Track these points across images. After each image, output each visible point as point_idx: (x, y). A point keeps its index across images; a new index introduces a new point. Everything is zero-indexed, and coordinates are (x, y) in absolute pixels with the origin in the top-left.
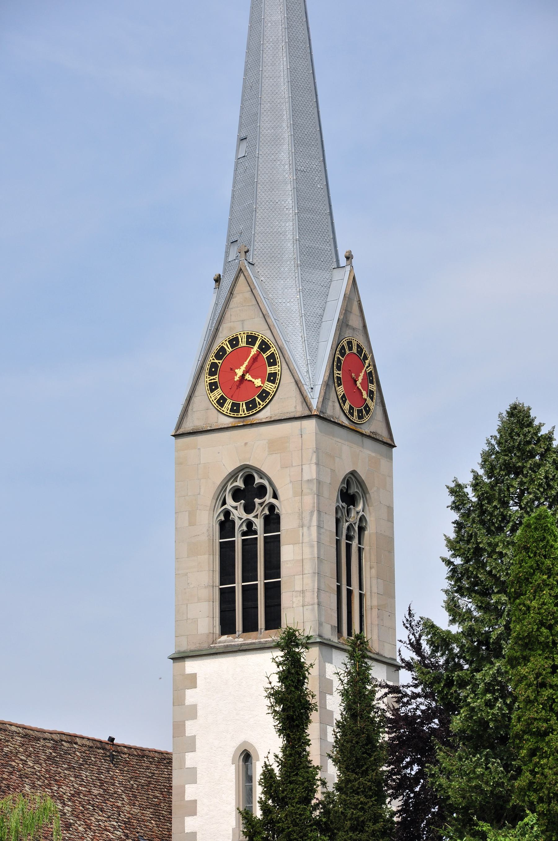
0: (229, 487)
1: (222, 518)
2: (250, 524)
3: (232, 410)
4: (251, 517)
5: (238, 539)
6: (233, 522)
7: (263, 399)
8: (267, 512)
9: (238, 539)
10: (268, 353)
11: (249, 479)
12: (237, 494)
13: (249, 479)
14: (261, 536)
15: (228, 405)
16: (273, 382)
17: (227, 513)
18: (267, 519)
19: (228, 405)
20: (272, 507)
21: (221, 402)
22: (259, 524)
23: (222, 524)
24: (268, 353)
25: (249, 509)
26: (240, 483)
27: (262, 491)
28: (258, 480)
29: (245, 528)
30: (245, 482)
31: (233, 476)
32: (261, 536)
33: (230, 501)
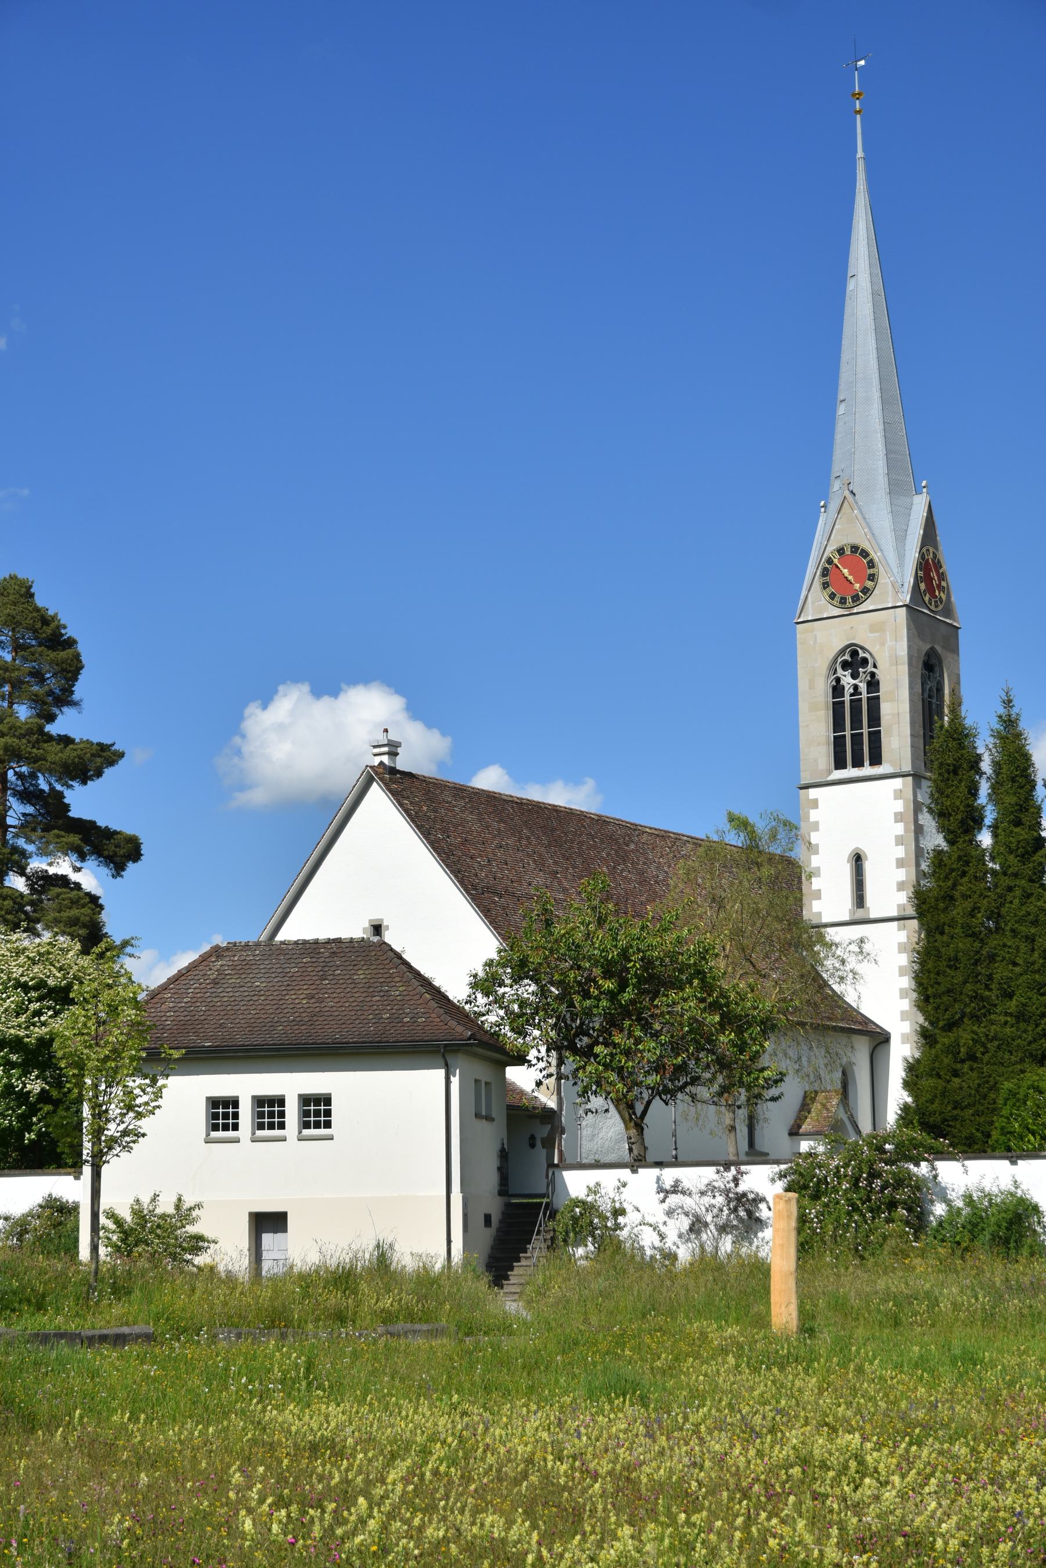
0: (840, 660)
1: (834, 683)
2: (856, 687)
3: (841, 603)
5: (847, 698)
6: (843, 687)
7: (865, 593)
8: (869, 678)
9: (847, 698)
10: (868, 559)
11: (854, 654)
12: (845, 665)
13: (854, 654)
14: (864, 695)
15: (837, 598)
16: (872, 580)
17: (838, 680)
19: (837, 598)
20: (873, 675)
22: (863, 687)
23: (834, 689)
24: (868, 559)
25: (854, 676)
26: (847, 657)
27: (865, 662)
28: (862, 654)
29: (852, 691)
31: (842, 652)
32: (864, 695)
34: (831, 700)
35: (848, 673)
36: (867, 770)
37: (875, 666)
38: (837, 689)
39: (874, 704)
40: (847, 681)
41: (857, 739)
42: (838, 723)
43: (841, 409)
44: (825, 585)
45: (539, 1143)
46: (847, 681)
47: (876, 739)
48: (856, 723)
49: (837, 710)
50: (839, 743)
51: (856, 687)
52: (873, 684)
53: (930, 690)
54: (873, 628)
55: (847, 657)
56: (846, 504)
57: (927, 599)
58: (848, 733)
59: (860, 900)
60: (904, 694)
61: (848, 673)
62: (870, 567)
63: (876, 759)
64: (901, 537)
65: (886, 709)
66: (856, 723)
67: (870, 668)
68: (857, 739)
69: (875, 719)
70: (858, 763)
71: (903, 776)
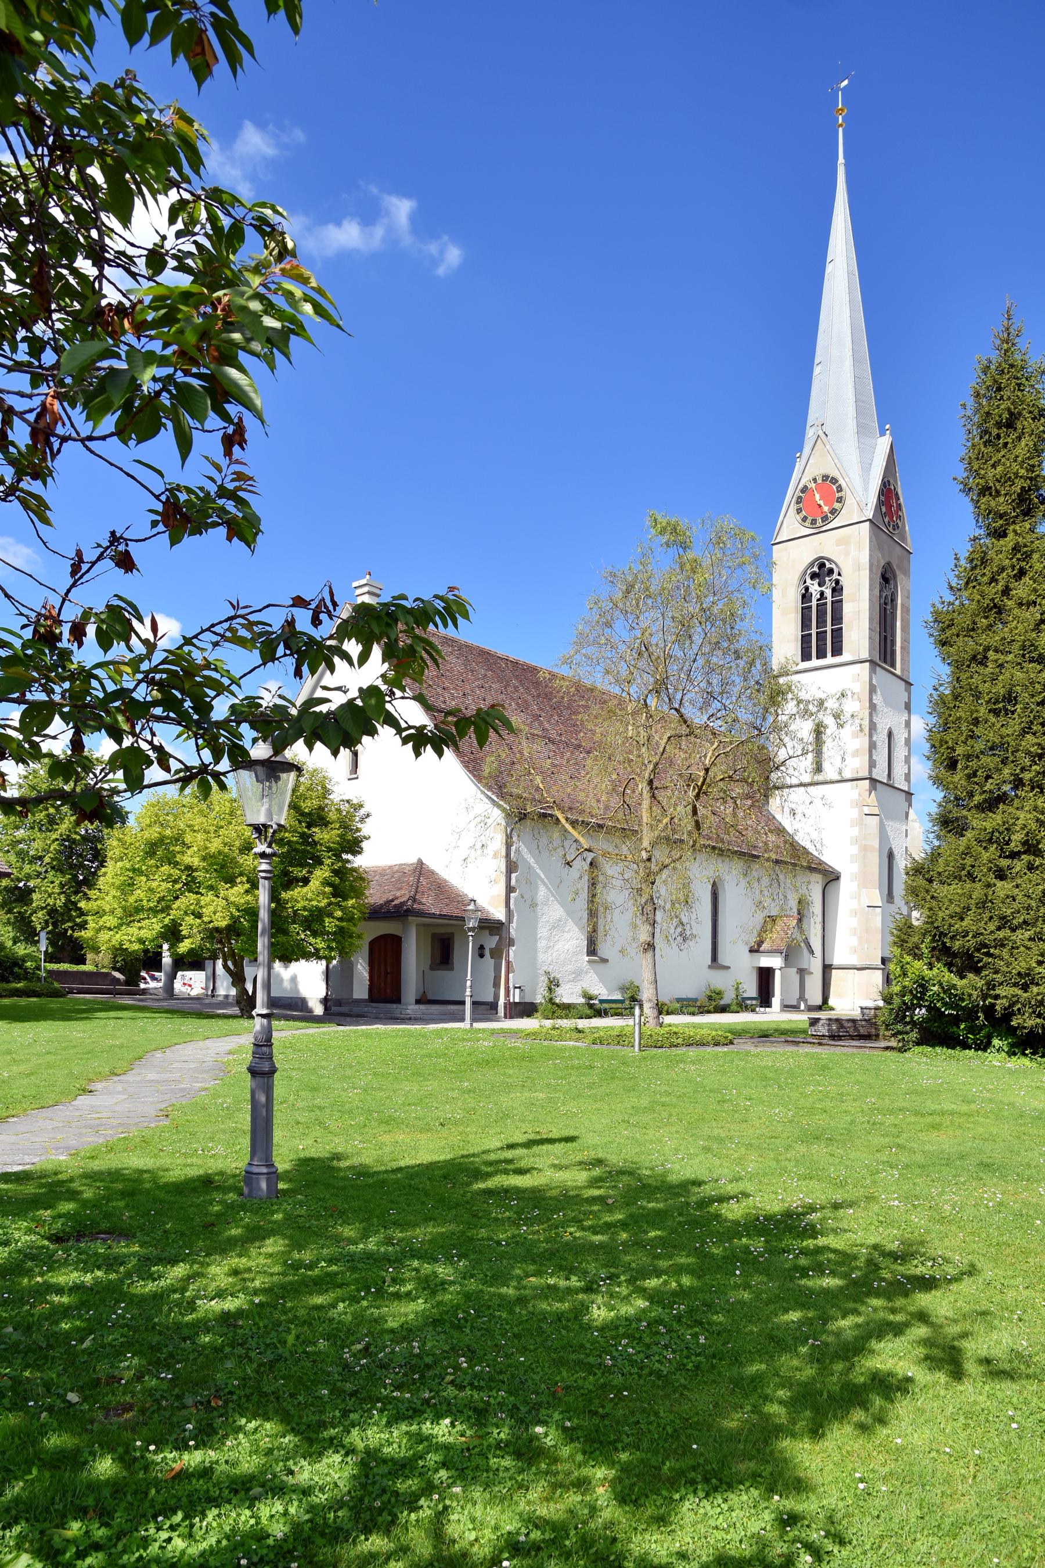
2: (822, 593)
4: (823, 589)
5: (814, 603)
8: (834, 585)
9: (814, 603)
11: (822, 566)
12: (814, 576)
13: (822, 566)
14: (829, 600)
15: (809, 521)
17: (807, 589)
18: (834, 590)
19: (809, 521)
20: (837, 582)
21: (804, 519)
22: (828, 593)
23: (804, 596)
26: (816, 569)
27: (831, 571)
28: (828, 565)
29: (818, 596)
30: (819, 568)
31: (812, 565)
32: (829, 600)
33: (809, 581)
34: (800, 606)
35: (816, 582)
36: (830, 660)
37: (839, 574)
38: (806, 596)
39: (837, 606)
40: (815, 588)
41: (821, 636)
42: (805, 624)
43: (817, 370)
44: (799, 511)
45: (487, 953)
46: (815, 588)
47: (837, 634)
48: (821, 621)
49: (805, 613)
50: (805, 640)
51: (822, 593)
52: (837, 589)
53: (886, 597)
54: (839, 542)
55: (816, 569)
56: (819, 440)
57: (886, 520)
58: (814, 631)
59: (818, 769)
60: (865, 605)
61: (816, 582)
62: (838, 492)
63: (837, 651)
64: (866, 468)
65: (848, 609)
66: (821, 621)
67: (835, 576)
68: (821, 636)
69: (837, 618)
70: (821, 655)
71: (861, 662)
